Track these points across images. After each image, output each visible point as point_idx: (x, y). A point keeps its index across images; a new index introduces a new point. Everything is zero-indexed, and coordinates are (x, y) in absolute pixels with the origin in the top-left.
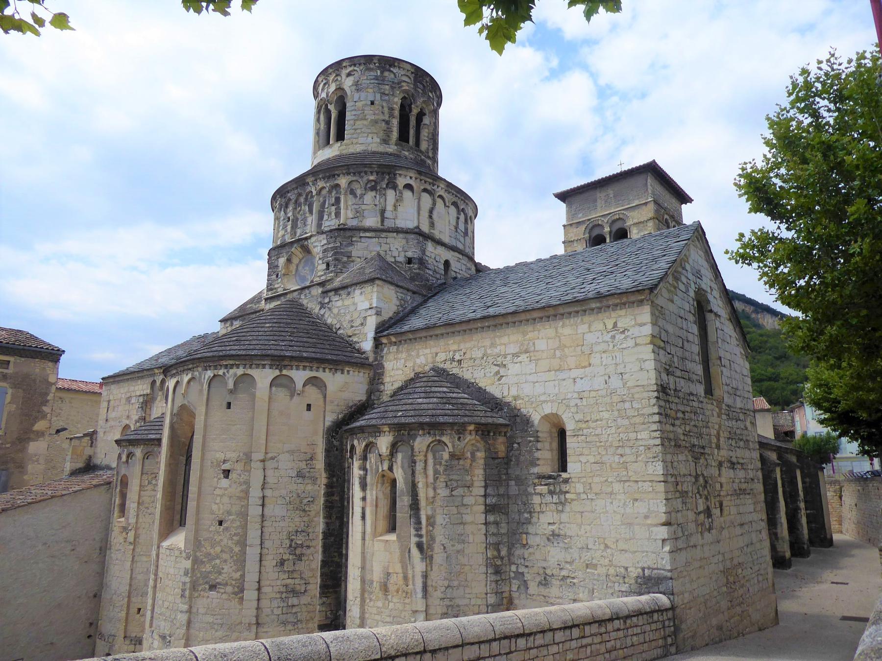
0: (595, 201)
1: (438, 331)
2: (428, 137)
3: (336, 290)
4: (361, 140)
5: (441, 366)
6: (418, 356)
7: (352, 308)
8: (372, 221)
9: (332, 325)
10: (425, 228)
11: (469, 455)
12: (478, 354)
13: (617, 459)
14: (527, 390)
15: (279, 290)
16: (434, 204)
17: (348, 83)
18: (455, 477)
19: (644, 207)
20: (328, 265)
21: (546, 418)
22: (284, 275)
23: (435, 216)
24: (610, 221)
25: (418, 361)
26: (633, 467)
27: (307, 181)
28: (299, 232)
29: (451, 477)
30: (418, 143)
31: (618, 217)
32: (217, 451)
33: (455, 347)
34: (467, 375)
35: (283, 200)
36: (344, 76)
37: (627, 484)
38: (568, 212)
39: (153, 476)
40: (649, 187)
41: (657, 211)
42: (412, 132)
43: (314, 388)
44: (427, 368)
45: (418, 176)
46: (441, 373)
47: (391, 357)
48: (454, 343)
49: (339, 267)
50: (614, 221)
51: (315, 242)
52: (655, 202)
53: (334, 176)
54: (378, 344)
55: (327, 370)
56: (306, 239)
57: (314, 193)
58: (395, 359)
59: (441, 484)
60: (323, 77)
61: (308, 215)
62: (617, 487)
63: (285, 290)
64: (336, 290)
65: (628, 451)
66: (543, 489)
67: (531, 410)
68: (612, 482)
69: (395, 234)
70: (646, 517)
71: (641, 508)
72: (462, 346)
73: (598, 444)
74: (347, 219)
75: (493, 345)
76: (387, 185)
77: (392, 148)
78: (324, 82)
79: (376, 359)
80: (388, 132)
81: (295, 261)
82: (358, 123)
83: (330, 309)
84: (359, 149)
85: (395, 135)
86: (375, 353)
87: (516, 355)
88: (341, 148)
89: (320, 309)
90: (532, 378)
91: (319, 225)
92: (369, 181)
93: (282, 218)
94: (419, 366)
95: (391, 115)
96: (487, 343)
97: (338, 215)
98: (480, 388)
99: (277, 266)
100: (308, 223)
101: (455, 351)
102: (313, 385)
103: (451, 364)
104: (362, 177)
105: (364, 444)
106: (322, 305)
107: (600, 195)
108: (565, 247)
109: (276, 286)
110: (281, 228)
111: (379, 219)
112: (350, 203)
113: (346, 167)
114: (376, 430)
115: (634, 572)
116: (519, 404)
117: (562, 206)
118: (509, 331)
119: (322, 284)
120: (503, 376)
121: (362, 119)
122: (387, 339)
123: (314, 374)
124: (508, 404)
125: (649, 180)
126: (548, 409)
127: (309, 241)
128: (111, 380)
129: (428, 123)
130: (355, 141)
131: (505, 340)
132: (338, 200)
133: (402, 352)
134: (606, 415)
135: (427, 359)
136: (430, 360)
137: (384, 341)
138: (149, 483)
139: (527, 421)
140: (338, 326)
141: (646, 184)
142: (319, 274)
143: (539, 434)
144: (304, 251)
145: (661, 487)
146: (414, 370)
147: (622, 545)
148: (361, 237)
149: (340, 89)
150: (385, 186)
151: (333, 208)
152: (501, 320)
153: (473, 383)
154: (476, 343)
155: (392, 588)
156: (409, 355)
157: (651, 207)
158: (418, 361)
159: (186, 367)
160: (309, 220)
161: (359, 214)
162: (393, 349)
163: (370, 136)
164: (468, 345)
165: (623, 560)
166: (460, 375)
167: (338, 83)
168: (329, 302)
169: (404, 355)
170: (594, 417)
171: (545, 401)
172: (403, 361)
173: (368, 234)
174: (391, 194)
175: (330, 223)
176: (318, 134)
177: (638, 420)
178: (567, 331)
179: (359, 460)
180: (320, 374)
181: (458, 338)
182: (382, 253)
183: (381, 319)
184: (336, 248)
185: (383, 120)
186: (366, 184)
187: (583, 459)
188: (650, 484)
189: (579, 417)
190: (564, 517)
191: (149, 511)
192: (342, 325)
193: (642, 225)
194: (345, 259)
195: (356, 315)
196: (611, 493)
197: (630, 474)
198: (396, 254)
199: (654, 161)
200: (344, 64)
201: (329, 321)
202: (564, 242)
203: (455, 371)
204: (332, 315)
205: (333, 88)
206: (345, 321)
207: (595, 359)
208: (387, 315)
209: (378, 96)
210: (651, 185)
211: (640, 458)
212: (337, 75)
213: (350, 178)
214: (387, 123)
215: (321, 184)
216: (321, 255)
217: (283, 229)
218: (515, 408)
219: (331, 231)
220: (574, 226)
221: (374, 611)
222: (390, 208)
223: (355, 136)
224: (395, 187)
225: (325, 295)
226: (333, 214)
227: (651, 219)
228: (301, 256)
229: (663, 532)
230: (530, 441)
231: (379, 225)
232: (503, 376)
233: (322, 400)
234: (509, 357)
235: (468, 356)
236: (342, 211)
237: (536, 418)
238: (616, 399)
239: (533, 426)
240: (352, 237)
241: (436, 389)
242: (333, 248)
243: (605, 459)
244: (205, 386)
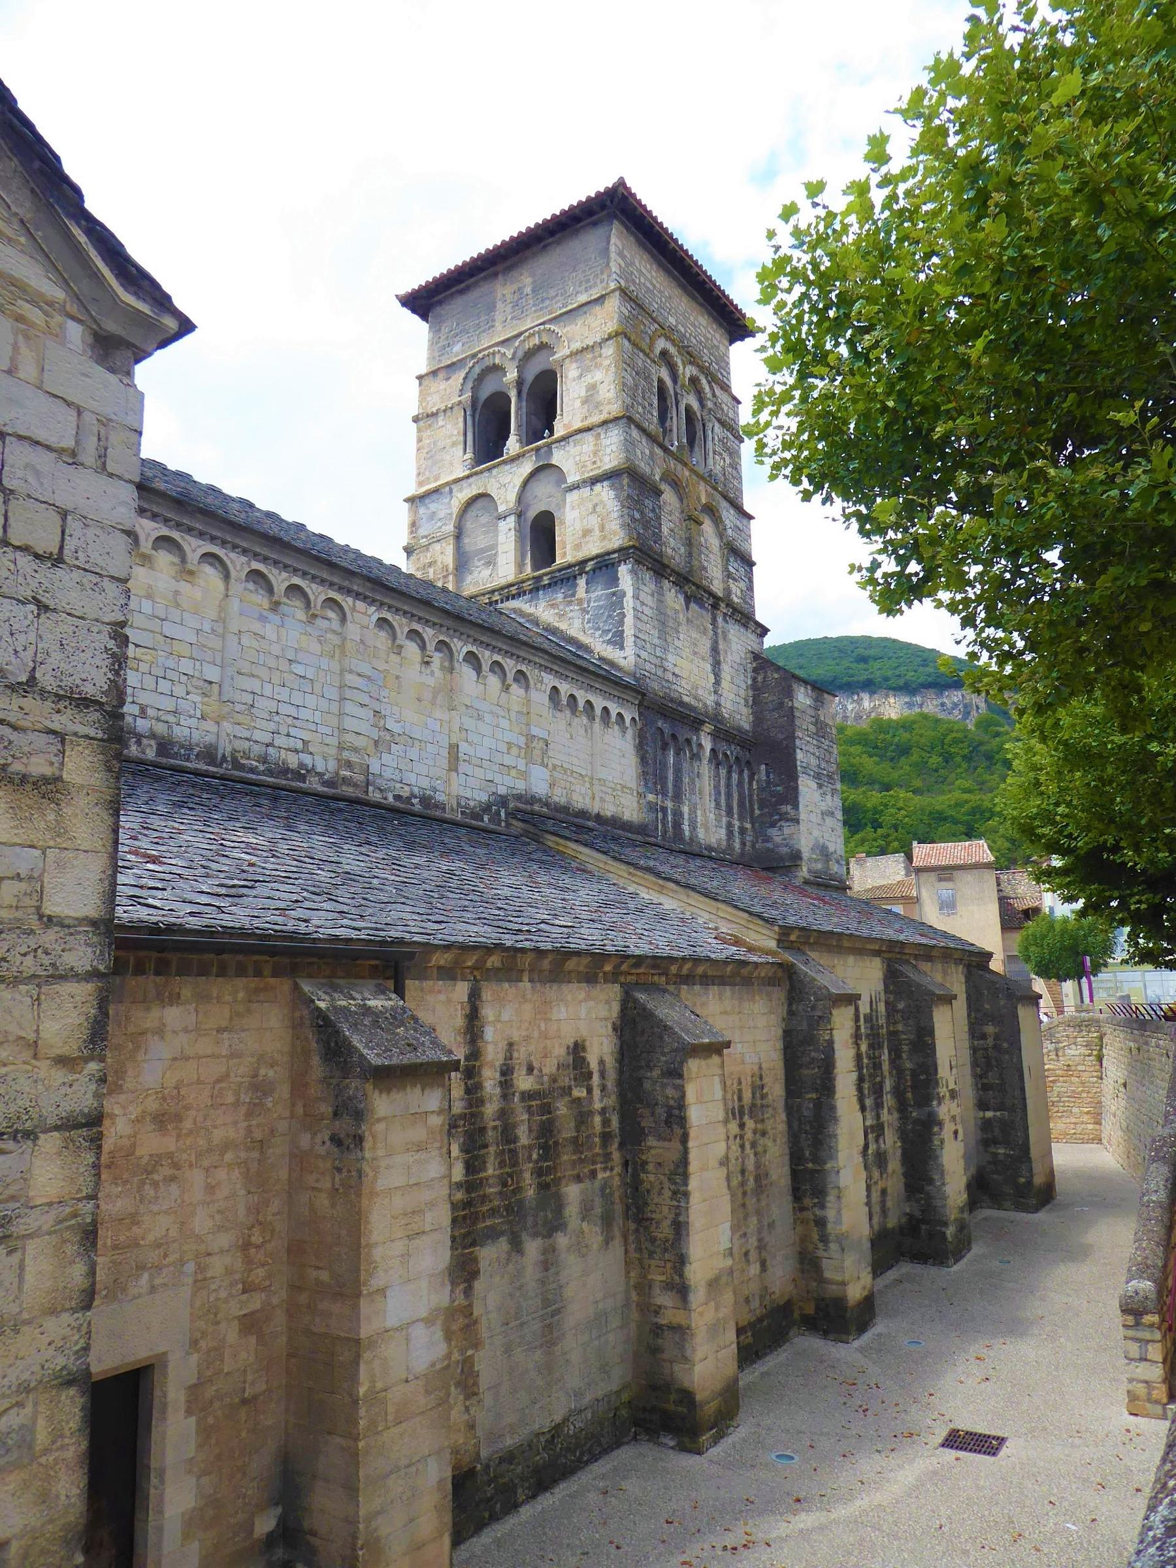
0: (492, 308)
19: (597, 309)
24: (520, 354)
31: (537, 341)
38: (433, 343)
40: (613, 256)
41: (624, 320)
50: (530, 354)
52: (624, 292)
107: (503, 290)
108: (419, 430)
117: (416, 327)
125: (613, 240)
141: (607, 250)
157: (614, 304)
193: (590, 356)
199: (621, 183)
202: (416, 420)
210: (621, 254)
220: (441, 375)
227: (610, 338)
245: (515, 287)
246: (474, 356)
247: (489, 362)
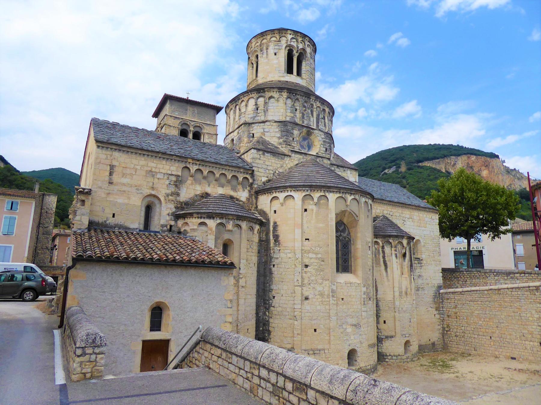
1: (384, 202)
6: (377, 209)
12: (398, 215)
17: (308, 50)
20: (326, 149)
24: (194, 125)
26: (436, 257)
27: (311, 97)
28: (306, 122)
33: (390, 210)
34: (394, 221)
35: (292, 97)
36: (306, 46)
39: (252, 242)
44: (381, 215)
53: (323, 104)
56: (313, 129)
57: (315, 107)
60: (292, 33)
61: (310, 115)
62: (433, 262)
65: (435, 253)
66: (416, 262)
72: (393, 210)
75: (402, 213)
87: (409, 219)
90: (413, 227)
91: (318, 126)
96: (400, 211)
97: (325, 125)
99: (293, 133)
105: (397, 242)
109: (293, 145)
110: (289, 111)
114: (403, 237)
115: (436, 285)
118: (406, 210)
128: (114, 147)
131: (405, 212)
132: (324, 118)
134: (430, 242)
136: (382, 212)
138: (250, 247)
142: (321, 152)
147: (434, 278)
149: (304, 49)
152: (404, 206)
155: (408, 293)
159: (349, 192)
160: (312, 119)
165: (434, 282)
170: (428, 242)
177: (436, 245)
178: (421, 215)
181: (391, 207)
187: (426, 254)
189: (424, 242)
190: (422, 270)
191: (250, 265)
200: (307, 38)
203: (390, 219)
205: (301, 46)
207: (427, 225)
212: (302, 41)
215: (318, 104)
219: (326, 133)
221: (403, 302)
226: (323, 123)
234: (406, 219)
238: (432, 238)
244: (363, 205)
245: (192, 109)
246: (182, 119)
247: (186, 123)
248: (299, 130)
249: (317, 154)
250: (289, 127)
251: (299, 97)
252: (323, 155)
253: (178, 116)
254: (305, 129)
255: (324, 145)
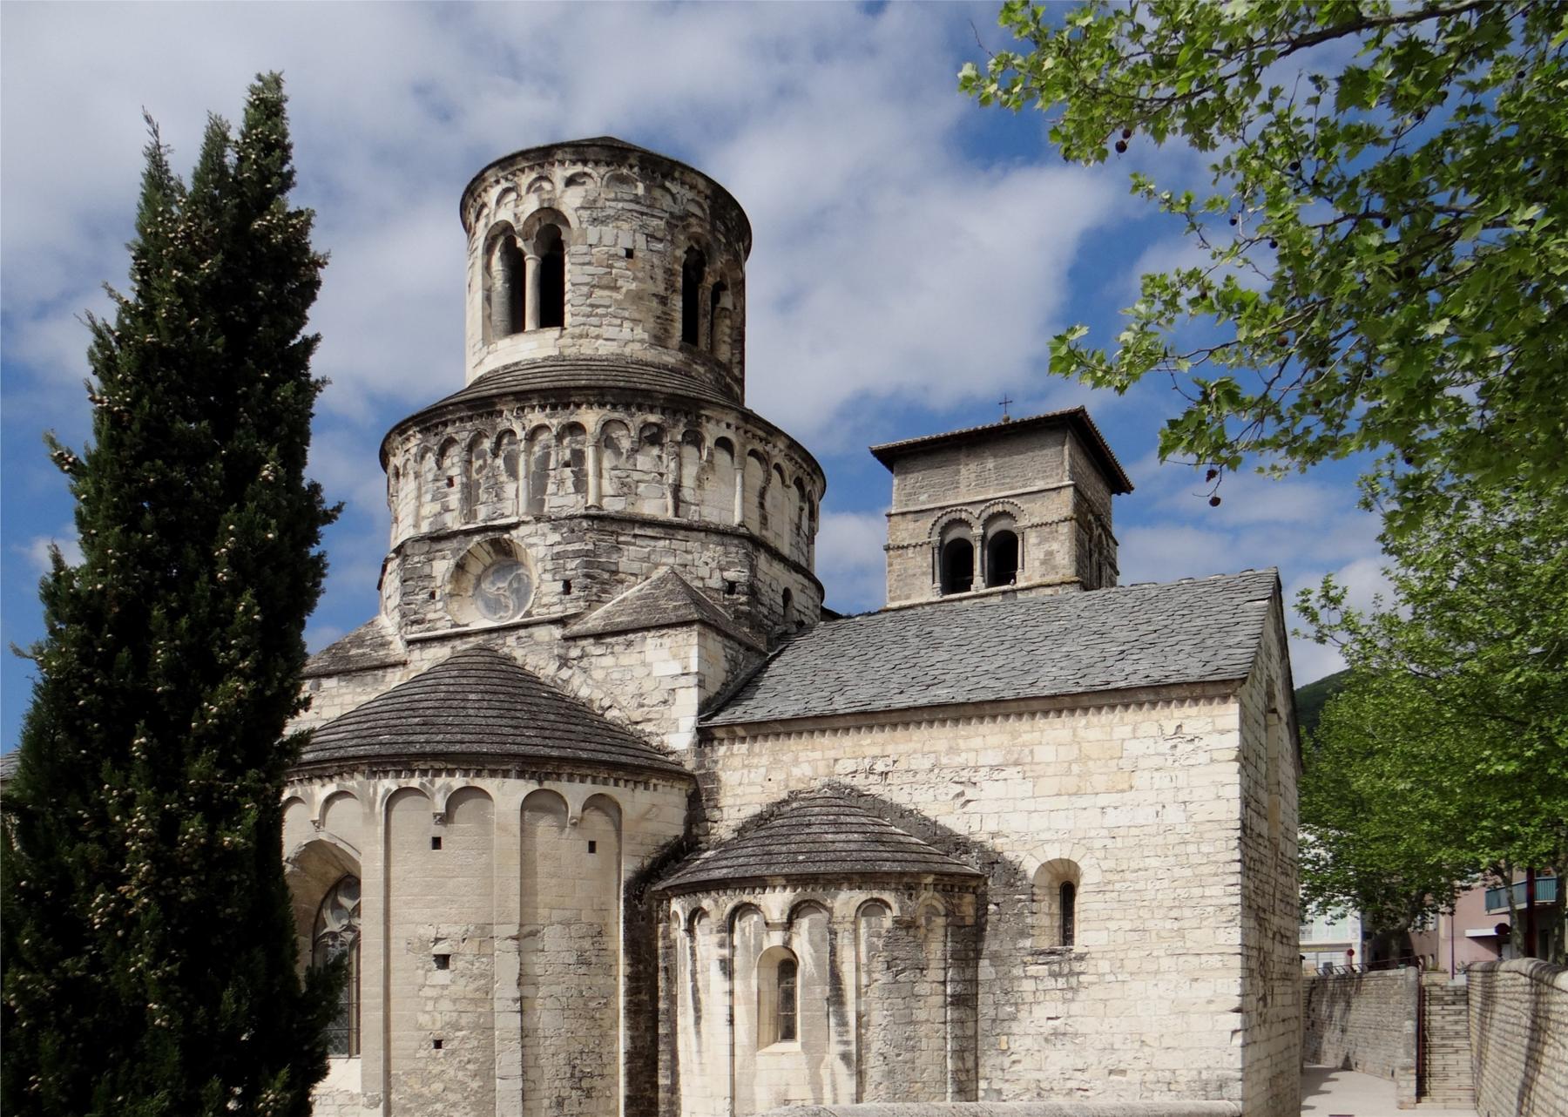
2: (730, 336)
3: (598, 636)
4: (608, 332)
5: (847, 780)
6: (796, 762)
7: (640, 672)
8: (655, 506)
9: (591, 701)
10: (755, 528)
11: (923, 921)
13: (1169, 924)
14: (1015, 823)
15: (439, 624)
16: (768, 480)
18: (902, 954)
21: (1048, 866)
22: (451, 595)
23: (768, 504)
25: (796, 772)
29: (896, 954)
30: (713, 348)
32: (417, 924)
33: (876, 751)
34: (900, 798)
37: (1182, 959)
42: (704, 325)
43: (599, 813)
44: (816, 784)
45: (741, 424)
46: (844, 799)
47: (736, 762)
48: (874, 743)
49: (594, 590)
51: (530, 535)
54: (705, 737)
55: (622, 783)
56: (508, 528)
58: (744, 766)
59: (879, 965)
62: (1166, 963)
63: (455, 625)
64: (598, 636)
67: (1023, 854)
68: (1158, 957)
69: (703, 534)
70: (1210, 1002)
71: (1203, 990)
72: (890, 749)
73: (1139, 904)
74: (600, 496)
76: (684, 435)
77: (671, 358)
78: (504, 184)
79: (700, 766)
80: (664, 320)
81: (475, 568)
82: (598, 293)
83: (585, 670)
84: (605, 349)
85: (677, 329)
86: (700, 754)
88: (562, 341)
89: (560, 668)
92: (647, 425)
93: (430, 477)
94: (799, 780)
95: (670, 286)
97: (580, 485)
98: (925, 819)
99: (430, 577)
100: (505, 495)
101: (875, 757)
102: (598, 808)
103: (867, 777)
104: (632, 415)
106: (564, 662)
109: (430, 616)
110: (428, 497)
111: (670, 501)
112: (606, 464)
113: (596, 392)
116: (999, 844)
119: (561, 622)
120: (969, 801)
121: (607, 287)
122: (728, 732)
123: (600, 789)
124: (981, 845)
126: (1053, 853)
127: (514, 533)
129: (730, 306)
130: (593, 331)
132: (578, 456)
133: (760, 755)
135: (815, 769)
136: (822, 769)
137: (719, 734)
139: (1013, 872)
140: (606, 703)
142: (545, 600)
143: (1036, 890)
144: (497, 552)
145: (1237, 962)
146: (787, 786)
148: (635, 536)
150: (679, 438)
151: (568, 470)
153: (911, 811)
154: (919, 746)
156: (776, 761)
158: (796, 772)
160: (510, 489)
161: (626, 488)
162: (740, 748)
163: (627, 324)
164: (903, 748)
166: (886, 797)
167: (546, 196)
168: (581, 657)
169: (765, 760)
171: (1047, 841)
172: (763, 770)
173: (650, 532)
174: (689, 452)
175: (562, 499)
176: (488, 299)
179: (719, 932)
180: (609, 790)
182: (678, 569)
183: (706, 695)
184: (587, 553)
185: (654, 295)
186: (642, 430)
187: (1112, 925)
188: (1220, 958)
192: (615, 700)
194: (606, 576)
195: (648, 685)
196: (1157, 972)
197: (1189, 944)
198: (704, 572)
201: (584, 693)
204: (590, 682)
206: (622, 694)
208: (713, 688)
209: (641, 241)
211: (1205, 923)
213: (607, 413)
214: (663, 301)
216: (549, 566)
217: (434, 500)
218: (994, 851)
222: (688, 481)
223: (594, 320)
224: (693, 438)
225: (571, 643)
228: (488, 561)
229: (1236, 1021)
230: (1020, 901)
231: (669, 515)
232: (969, 801)
233: (613, 836)
235: (902, 765)
236: (591, 480)
237: (1031, 867)
239: (1025, 877)
240: (618, 534)
241: (848, 819)
242: (577, 554)
243: (1149, 925)
248: (455, 552)
249: (528, 614)
250: (416, 559)
251: (450, 429)
252: (553, 609)
253: (924, 507)
254: (477, 538)
255: (555, 571)
